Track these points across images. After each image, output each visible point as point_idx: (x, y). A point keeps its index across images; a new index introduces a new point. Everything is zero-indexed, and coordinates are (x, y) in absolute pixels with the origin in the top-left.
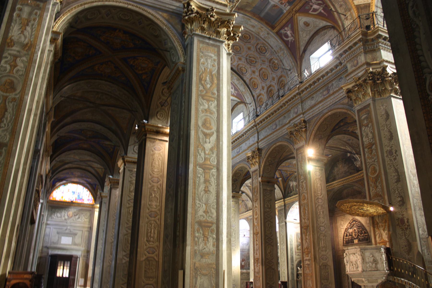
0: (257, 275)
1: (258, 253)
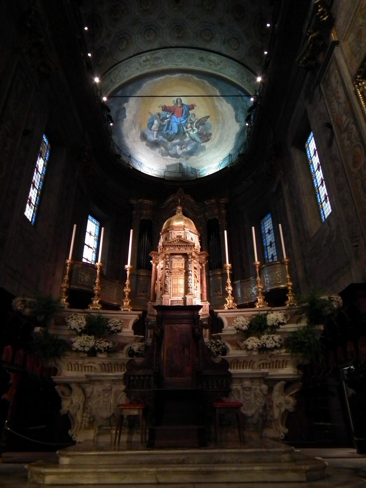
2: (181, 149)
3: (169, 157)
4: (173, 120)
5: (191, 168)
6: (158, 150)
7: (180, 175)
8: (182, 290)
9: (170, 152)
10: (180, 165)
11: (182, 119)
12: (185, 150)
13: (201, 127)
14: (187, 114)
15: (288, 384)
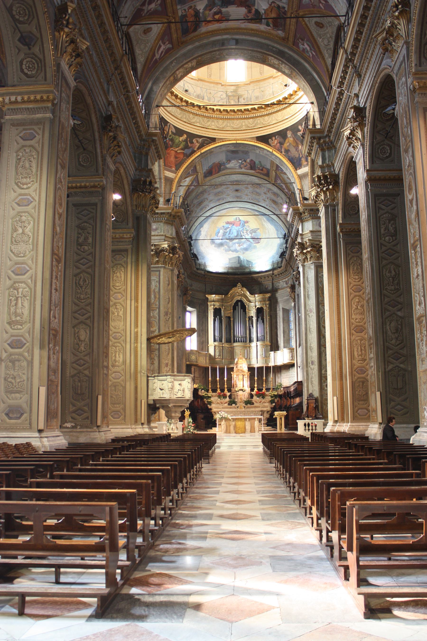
1: (57, 316)
2: (239, 246)
3: (231, 252)
5: (247, 261)
7: (238, 265)
8: (242, 386)
9: (231, 248)
10: (239, 257)
11: (240, 227)
12: (242, 247)
13: (253, 234)
14: (243, 226)
15: (268, 412)
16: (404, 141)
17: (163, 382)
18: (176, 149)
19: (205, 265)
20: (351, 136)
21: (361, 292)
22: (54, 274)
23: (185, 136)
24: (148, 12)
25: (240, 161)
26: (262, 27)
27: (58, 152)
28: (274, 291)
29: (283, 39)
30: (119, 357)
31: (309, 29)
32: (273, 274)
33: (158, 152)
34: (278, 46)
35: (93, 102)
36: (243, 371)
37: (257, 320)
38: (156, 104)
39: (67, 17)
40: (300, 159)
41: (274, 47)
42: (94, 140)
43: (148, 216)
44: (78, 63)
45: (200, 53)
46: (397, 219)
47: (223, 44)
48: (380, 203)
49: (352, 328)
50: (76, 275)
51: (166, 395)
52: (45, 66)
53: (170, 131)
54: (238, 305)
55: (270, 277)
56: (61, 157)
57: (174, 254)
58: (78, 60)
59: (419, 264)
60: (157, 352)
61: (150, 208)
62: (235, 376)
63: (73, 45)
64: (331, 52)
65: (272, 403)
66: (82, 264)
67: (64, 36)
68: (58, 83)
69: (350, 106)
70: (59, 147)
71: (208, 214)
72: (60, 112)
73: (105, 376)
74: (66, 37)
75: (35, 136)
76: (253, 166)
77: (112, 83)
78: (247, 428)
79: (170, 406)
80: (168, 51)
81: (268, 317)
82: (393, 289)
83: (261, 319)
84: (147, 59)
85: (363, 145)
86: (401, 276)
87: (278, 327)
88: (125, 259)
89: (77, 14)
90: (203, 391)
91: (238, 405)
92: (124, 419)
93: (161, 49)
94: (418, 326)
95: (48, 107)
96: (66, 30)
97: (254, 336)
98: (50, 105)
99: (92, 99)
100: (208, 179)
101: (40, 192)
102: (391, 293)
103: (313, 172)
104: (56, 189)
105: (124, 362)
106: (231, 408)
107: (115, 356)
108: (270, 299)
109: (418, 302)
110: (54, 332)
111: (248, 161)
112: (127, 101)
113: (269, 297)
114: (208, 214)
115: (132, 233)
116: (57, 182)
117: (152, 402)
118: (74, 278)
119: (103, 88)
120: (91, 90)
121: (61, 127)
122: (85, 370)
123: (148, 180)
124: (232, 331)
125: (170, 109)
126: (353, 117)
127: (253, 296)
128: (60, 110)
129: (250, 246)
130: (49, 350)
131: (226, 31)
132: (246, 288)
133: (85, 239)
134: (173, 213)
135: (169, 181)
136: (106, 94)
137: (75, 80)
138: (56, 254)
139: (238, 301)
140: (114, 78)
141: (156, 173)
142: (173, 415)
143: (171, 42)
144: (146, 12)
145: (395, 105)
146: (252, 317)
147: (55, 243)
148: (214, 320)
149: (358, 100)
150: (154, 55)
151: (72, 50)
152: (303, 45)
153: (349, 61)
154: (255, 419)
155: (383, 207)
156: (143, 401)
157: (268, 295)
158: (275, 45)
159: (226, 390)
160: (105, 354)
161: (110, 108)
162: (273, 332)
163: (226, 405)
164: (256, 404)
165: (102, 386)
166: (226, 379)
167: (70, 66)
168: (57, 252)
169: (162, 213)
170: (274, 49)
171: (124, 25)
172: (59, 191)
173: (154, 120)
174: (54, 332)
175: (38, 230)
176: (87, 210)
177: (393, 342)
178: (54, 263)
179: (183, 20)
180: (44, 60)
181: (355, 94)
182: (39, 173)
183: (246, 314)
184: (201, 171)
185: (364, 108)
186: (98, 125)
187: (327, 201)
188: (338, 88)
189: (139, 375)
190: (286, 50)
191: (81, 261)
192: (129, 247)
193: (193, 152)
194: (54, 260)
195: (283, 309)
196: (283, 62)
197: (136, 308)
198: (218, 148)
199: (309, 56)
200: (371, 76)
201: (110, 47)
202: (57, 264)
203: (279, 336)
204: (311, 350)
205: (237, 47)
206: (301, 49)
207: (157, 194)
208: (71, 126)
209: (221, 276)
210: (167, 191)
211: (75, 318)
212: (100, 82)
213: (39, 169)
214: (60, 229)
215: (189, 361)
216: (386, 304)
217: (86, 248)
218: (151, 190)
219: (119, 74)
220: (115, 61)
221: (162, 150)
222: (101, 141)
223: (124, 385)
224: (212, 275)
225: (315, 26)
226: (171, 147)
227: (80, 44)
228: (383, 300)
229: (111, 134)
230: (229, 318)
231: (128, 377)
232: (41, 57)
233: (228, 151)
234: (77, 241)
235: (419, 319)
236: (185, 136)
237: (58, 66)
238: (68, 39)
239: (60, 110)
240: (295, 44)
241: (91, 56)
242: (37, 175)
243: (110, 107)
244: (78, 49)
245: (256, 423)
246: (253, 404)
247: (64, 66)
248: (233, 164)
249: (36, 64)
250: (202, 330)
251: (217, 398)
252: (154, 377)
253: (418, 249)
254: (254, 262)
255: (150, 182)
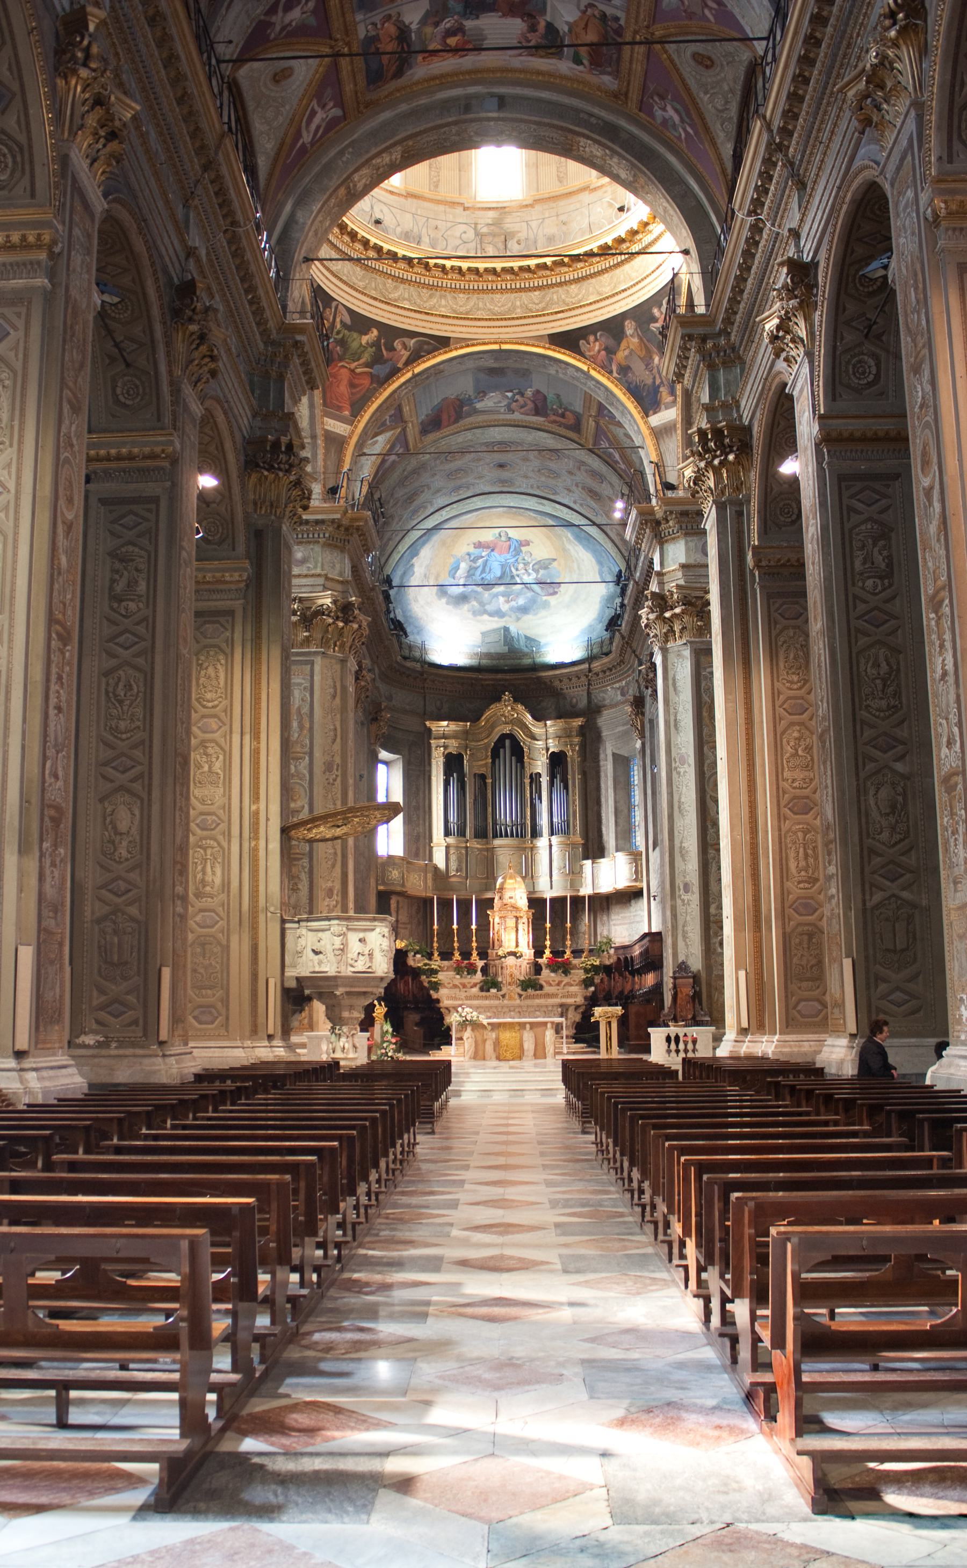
0: (50, 923)
1: (60, 773)
2: (508, 602)
3: (486, 617)
4: (493, 558)
5: (526, 637)
6: (466, 607)
7: (505, 649)
9: (488, 607)
10: (506, 629)
11: (508, 556)
12: (513, 603)
13: (542, 572)
14: (518, 552)
15: (577, 1007)
16: (911, 344)
17: (320, 934)
18: (353, 366)
19: (423, 649)
20: (781, 334)
21: (805, 715)
22: (54, 670)
23: (375, 332)
24: (283, 28)
25: (509, 394)
26: (564, 66)
27: (62, 373)
28: (592, 711)
29: (616, 95)
30: (214, 873)
31: (677, 70)
32: (590, 670)
33: (307, 372)
34: (603, 114)
35: (148, 249)
36: (515, 908)
37: (551, 784)
38: (303, 254)
39: (85, 42)
40: (655, 390)
41: (591, 115)
42: (153, 341)
43: (284, 528)
44: (112, 155)
45: (411, 130)
46: (893, 535)
47: (467, 108)
48: (851, 497)
49: (783, 803)
50: (107, 674)
51: (329, 967)
52: (32, 162)
53: (338, 320)
54: (504, 747)
55: (583, 679)
56: (71, 384)
57: (346, 622)
58: (114, 146)
59: (948, 645)
60: (305, 862)
61: (289, 509)
62: (497, 920)
63: (99, 111)
64: (732, 127)
65: (587, 987)
66: (121, 646)
67: (79, 89)
68: (64, 204)
69: (779, 260)
70: (67, 359)
71: (430, 523)
72: (68, 275)
73: (178, 919)
74: (83, 91)
75: (8, 334)
76: (540, 406)
77: (196, 202)
78: (526, 1046)
79: (338, 993)
80: (332, 124)
81: (578, 777)
82: (885, 707)
83: (562, 781)
84: (282, 144)
85: (809, 355)
86: (902, 675)
87: (603, 800)
88: (228, 634)
89: (110, 34)
90: (419, 956)
91: (504, 991)
92: (226, 1025)
93: (317, 120)
94: (945, 797)
95: (39, 263)
96: (84, 73)
97: (544, 821)
98: (43, 256)
99: (146, 242)
100: (431, 437)
101: (19, 471)
102: (877, 717)
103: (688, 421)
104: (58, 464)
105: (226, 885)
106: (486, 998)
107: (204, 871)
108: (582, 731)
109: (945, 740)
110: (52, 812)
111: (529, 393)
112: (233, 248)
113: (581, 727)
114: (430, 523)
115: (245, 570)
116: (62, 444)
117: (293, 984)
118: (104, 680)
119: (173, 216)
120: (145, 220)
121: (70, 310)
122: (130, 904)
123: (284, 440)
124: (490, 809)
125: (337, 266)
126: (785, 286)
127: (541, 724)
128: (68, 269)
129: (533, 601)
130: (42, 855)
131: (475, 76)
132: (522, 704)
133: (129, 586)
134: (345, 522)
135: (336, 443)
136: (182, 229)
137: (105, 195)
138: (58, 622)
139: (503, 737)
140: (199, 191)
141: (304, 423)
142: (346, 1014)
143: (340, 104)
144: (278, 28)
145: (889, 258)
146: (539, 775)
147: (55, 594)
148: (447, 784)
149: (797, 245)
150: (298, 135)
151: (99, 121)
152: (664, 109)
153: (776, 148)
154: (545, 1024)
155: (860, 506)
156: (272, 982)
157: (578, 722)
158: (596, 111)
159: (475, 953)
160: (178, 867)
161: (192, 264)
162: (590, 812)
163: (475, 990)
164: (547, 989)
165: (170, 944)
166: (474, 927)
167: (94, 161)
168: (60, 616)
169: (317, 522)
170: (593, 120)
171: (224, 61)
172: (67, 466)
173: (299, 293)
174: (52, 812)
175: (15, 562)
176: (136, 515)
177: (885, 836)
178: (54, 644)
179: (370, 48)
180: (30, 147)
181: (790, 230)
182: (16, 423)
183: (523, 767)
184: (414, 419)
185: (814, 264)
186: (161, 307)
187: (723, 493)
188: (749, 214)
189: (262, 918)
190: (623, 123)
191: (121, 639)
192: (238, 604)
193: (395, 372)
194: (54, 635)
195: (614, 755)
196: (614, 152)
197: (256, 753)
198: (455, 362)
199: (679, 138)
200: (830, 186)
201: (190, 116)
202: (60, 644)
203: (604, 821)
204: (682, 856)
205: (502, 115)
206: (659, 121)
207: (307, 474)
208: (95, 304)
209: (462, 674)
210: (331, 468)
211: (104, 777)
212: (167, 202)
213: (17, 413)
214: (68, 561)
215: (384, 883)
216: (866, 744)
217: (132, 606)
218: (291, 466)
219: (212, 182)
220: (202, 149)
221: (318, 366)
222: (168, 344)
223: (225, 942)
224: (441, 671)
225: (692, 63)
226: (341, 359)
227: (116, 109)
228: (858, 733)
229: (193, 328)
230: (483, 777)
231: (234, 921)
232: (22, 139)
233: (480, 370)
234: (111, 589)
235: (946, 780)
236: (375, 332)
237: (64, 160)
238: (87, 96)
239: (68, 269)
240: (643, 106)
241: (143, 136)
242: (12, 427)
243: (191, 260)
244: (112, 120)
245: (549, 1034)
246: (541, 988)
247: (79, 161)
248: (492, 401)
249: (9, 156)
250: (417, 808)
251: (452, 973)
252: (298, 922)
253: (946, 610)
254: (543, 641)
255: (290, 447)
